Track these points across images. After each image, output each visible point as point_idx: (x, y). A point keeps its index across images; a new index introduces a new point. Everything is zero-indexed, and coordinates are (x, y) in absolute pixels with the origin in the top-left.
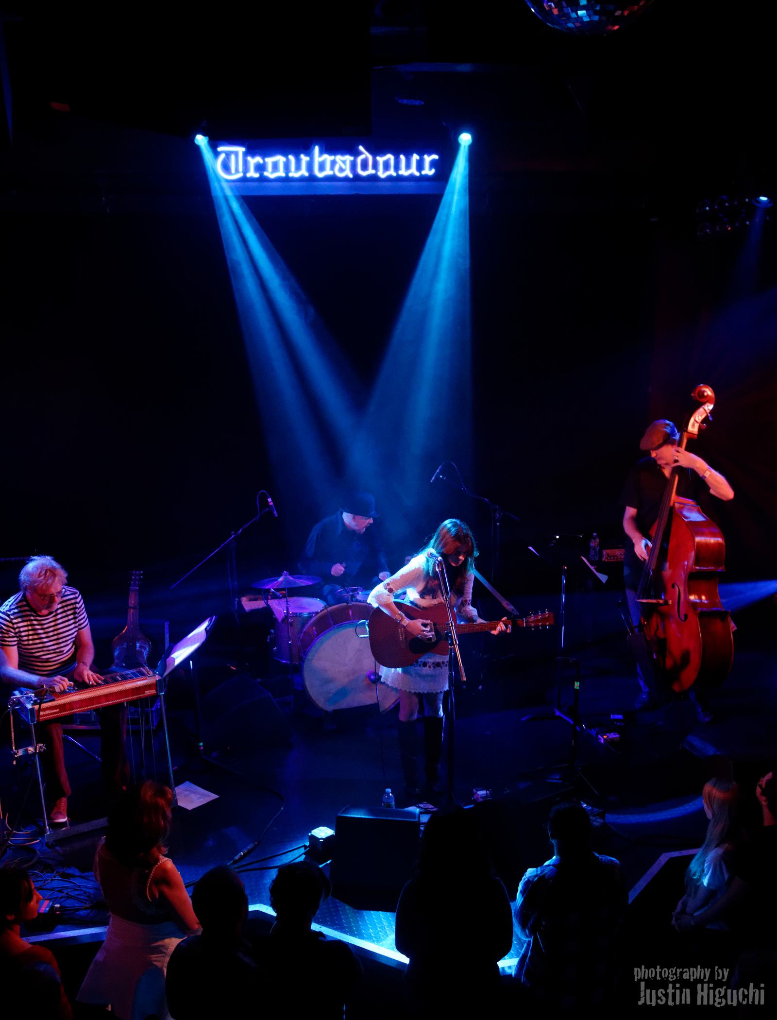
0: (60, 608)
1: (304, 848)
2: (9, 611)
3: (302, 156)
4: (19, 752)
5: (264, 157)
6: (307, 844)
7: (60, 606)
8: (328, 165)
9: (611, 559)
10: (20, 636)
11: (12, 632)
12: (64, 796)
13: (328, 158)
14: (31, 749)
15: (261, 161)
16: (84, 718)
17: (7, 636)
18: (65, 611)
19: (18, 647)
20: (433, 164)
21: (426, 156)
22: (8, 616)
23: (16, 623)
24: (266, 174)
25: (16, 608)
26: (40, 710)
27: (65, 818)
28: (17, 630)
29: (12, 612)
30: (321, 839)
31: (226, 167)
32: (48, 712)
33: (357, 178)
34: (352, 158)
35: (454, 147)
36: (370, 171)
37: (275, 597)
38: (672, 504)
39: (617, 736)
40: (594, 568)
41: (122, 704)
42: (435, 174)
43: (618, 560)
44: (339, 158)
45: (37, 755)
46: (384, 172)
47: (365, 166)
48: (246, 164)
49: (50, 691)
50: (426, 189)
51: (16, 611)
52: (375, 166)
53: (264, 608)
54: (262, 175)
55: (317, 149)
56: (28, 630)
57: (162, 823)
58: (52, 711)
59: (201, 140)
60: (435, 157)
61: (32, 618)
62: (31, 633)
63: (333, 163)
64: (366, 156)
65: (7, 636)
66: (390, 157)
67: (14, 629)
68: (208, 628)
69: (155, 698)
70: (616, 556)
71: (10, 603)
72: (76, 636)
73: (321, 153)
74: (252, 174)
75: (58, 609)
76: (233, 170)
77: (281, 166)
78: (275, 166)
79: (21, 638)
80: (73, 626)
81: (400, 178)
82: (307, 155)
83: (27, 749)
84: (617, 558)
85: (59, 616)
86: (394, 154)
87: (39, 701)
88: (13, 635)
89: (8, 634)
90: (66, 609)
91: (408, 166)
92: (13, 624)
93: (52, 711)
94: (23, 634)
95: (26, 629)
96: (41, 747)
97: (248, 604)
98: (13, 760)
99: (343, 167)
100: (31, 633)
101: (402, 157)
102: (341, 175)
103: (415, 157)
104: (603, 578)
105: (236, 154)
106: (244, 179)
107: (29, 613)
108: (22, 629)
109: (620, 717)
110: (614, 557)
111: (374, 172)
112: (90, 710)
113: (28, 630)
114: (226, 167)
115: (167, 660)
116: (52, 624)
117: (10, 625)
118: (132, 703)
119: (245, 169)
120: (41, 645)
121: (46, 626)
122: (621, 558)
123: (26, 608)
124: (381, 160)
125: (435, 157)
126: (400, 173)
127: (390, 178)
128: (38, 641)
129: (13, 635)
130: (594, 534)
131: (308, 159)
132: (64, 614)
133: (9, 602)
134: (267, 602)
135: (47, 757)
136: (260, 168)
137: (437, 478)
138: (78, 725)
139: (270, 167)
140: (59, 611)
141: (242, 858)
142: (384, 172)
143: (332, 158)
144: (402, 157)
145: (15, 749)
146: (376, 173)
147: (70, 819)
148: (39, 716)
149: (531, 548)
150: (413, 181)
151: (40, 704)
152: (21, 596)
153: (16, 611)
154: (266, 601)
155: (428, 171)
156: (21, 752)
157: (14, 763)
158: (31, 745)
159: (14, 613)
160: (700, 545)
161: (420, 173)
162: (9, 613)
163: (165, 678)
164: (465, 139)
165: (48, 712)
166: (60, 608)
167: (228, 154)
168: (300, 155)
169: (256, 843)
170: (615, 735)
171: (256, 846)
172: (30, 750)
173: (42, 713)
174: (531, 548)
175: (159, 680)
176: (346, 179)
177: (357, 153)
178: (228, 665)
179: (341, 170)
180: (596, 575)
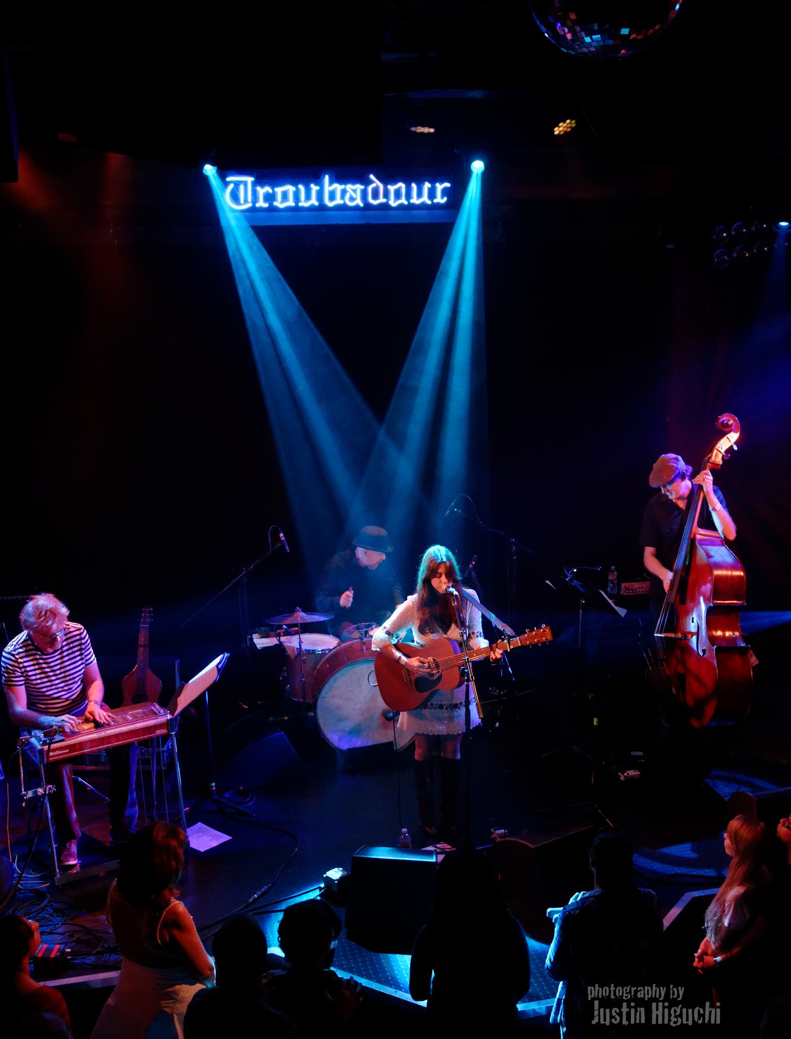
0: (66, 645)
1: (318, 890)
2: (15, 650)
3: (312, 185)
4: (29, 793)
5: (273, 186)
6: (322, 885)
7: (64, 643)
8: (338, 195)
9: (629, 592)
10: (27, 675)
11: (18, 672)
12: (74, 838)
13: (338, 187)
14: (40, 791)
15: (271, 191)
16: (94, 758)
17: (13, 675)
18: (71, 648)
19: (25, 686)
20: (445, 192)
21: (437, 185)
22: (13, 655)
23: (21, 663)
24: (275, 204)
25: (21, 648)
26: (49, 750)
27: (75, 860)
28: (23, 670)
29: (17, 652)
30: (336, 880)
31: (235, 197)
32: (57, 753)
33: (368, 207)
34: (363, 187)
35: (468, 173)
36: (382, 200)
37: (287, 633)
38: (692, 537)
39: (638, 773)
40: (612, 602)
41: (132, 744)
42: (447, 202)
43: (638, 593)
44: (349, 187)
45: (46, 797)
46: (395, 202)
47: (375, 195)
48: (255, 193)
49: (59, 731)
50: (438, 217)
51: (21, 650)
53: (276, 645)
54: (271, 205)
55: (327, 177)
56: (35, 670)
57: (174, 863)
58: (62, 752)
59: (209, 170)
60: (447, 185)
61: (38, 657)
62: (38, 672)
63: (344, 192)
64: (377, 184)
65: (13, 675)
66: (401, 185)
67: (20, 668)
68: (220, 666)
69: (166, 738)
70: (635, 590)
71: (14, 643)
72: (83, 672)
73: (331, 183)
74: (262, 204)
75: (63, 647)
76: (242, 201)
77: (291, 196)
78: (285, 196)
79: (28, 678)
80: (80, 662)
81: (412, 207)
82: (316, 184)
83: (37, 791)
84: (636, 592)
85: (65, 654)
86: (404, 182)
87: (48, 741)
88: (20, 674)
89: (14, 674)
90: (71, 645)
91: (420, 195)
92: (19, 663)
93: (62, 752)
94: (30, 673)
95: (32, 668)
96: (50, 789)
97: (260, 642)
98: (23, 802)
99: (354, 196)
100: (38, 672)
101: (414, 185)
103: (427, 185)
104: (622, 612)
105: (245, 183)
106: (253, 209)
107: (34, 652)
108: (28, 669)
109: (640, 753)
110: (632, 590)
111: (385, 200)
112: (100, 750)
113: (35, 670)
114: (235, 197)
115: (178, 699)
116: (59, 662)
117: (16, 664)
118: (143, 743)
119: (254, 199)
120: (49, 684)
121: (52, 664)
122: (640, 591)
123: (31, 647)
124: (392, 188)
125: (447, 185)
126: (412, 201)
127: (401, 207)
128: (46, 680)
129: (20, 674)
130: (612, 567)
131: (318, 188)
132: (70, 651)
133: (14, 641)
134: (280, 638)
135: (57, 799)
137: (452, 512)
138: (89, 766)
139: (279, 197)
140: (65, 649)
141: (255, 900)
142: (395, 202)
143: (343, 187)
144: (414, 185)
145: (25, 791)
146: (387, 202)
147: (80, 861)
148: (48, 757)
149: (548, 582)
150: (426, 209)
151: (49, 744)
152: (26, 635)
153: (21, 650)
154: (278, 638)
155: (440, 200)
156: (30, 794)
157: (24, 805)
158: (39, 786)
159: (19, 653)
160: (719, 578)
161: (432, 201)
162: (13, 653)
163: (176, 716)
164: (478, 166)
165: (57, 753)
166: (66, 645)
167: (237, 184)
168: (310, 184)
169: (270, 885)
170: (635, 772)
171: (270, 888)
172: (39, 792)
173: (51, 754)
174: (548, 582)
175: (171, 719)
176: (357, 208)
177: (367, 182)
178: (240, 703)
179: (352, 199)
180: (614, 608)
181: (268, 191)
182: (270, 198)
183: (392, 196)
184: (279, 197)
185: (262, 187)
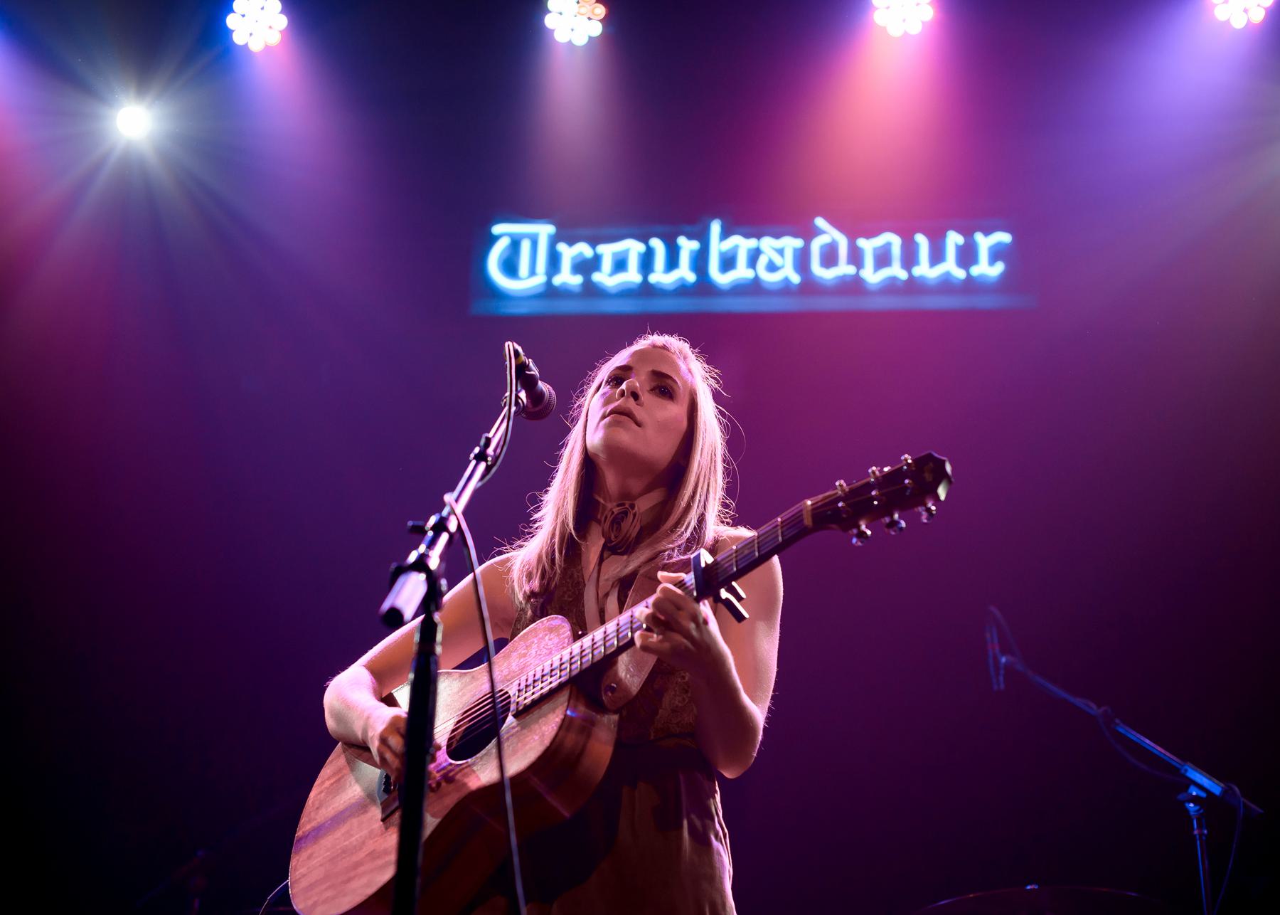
3: (682, 241)
5: (594, 242)
8: (742, 259)
13: (742, 244)
20: (997, 254)
21: (979, 237)
24: (596, 277)
33: (809, 286)
34: (799, 243)
36: (844, 269)
44: (767, 243)
47: (830, 258)
52: (856, 257)
55: (716, 227)
60: (1004, 237)
73: (725, 234)
74: (568, 278)
78: (620, 265)
81: (914, 286)
82: (690, 237)
91: (937, 256)
99: (778, 260)
101: (922, 240)
102: (769, 278)
103: (954, 239)
106: (550, 292)
111: (851, 270)
124: (868, 246)
125: (1004, 237)
126: (917, 271)
127: (891, 287)
131: (695, 245)
136: (586, 267)
139: (607, 264)
143: (752, 243)
144: (922, 240)
155: (988, 269)
176: (786, 289)
177: (808, 233)
179: (772, 267)
181: (581, 254)
182: (586, 267)
183: (869, 261)
184: (607, 264)
185: (571, 242)
